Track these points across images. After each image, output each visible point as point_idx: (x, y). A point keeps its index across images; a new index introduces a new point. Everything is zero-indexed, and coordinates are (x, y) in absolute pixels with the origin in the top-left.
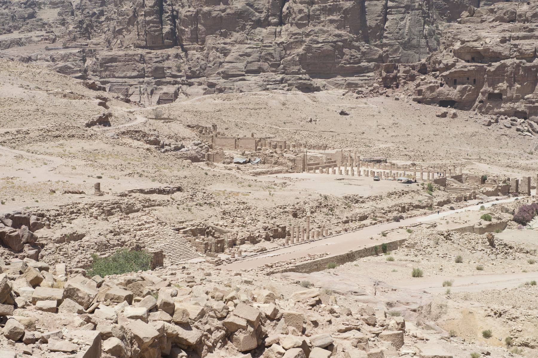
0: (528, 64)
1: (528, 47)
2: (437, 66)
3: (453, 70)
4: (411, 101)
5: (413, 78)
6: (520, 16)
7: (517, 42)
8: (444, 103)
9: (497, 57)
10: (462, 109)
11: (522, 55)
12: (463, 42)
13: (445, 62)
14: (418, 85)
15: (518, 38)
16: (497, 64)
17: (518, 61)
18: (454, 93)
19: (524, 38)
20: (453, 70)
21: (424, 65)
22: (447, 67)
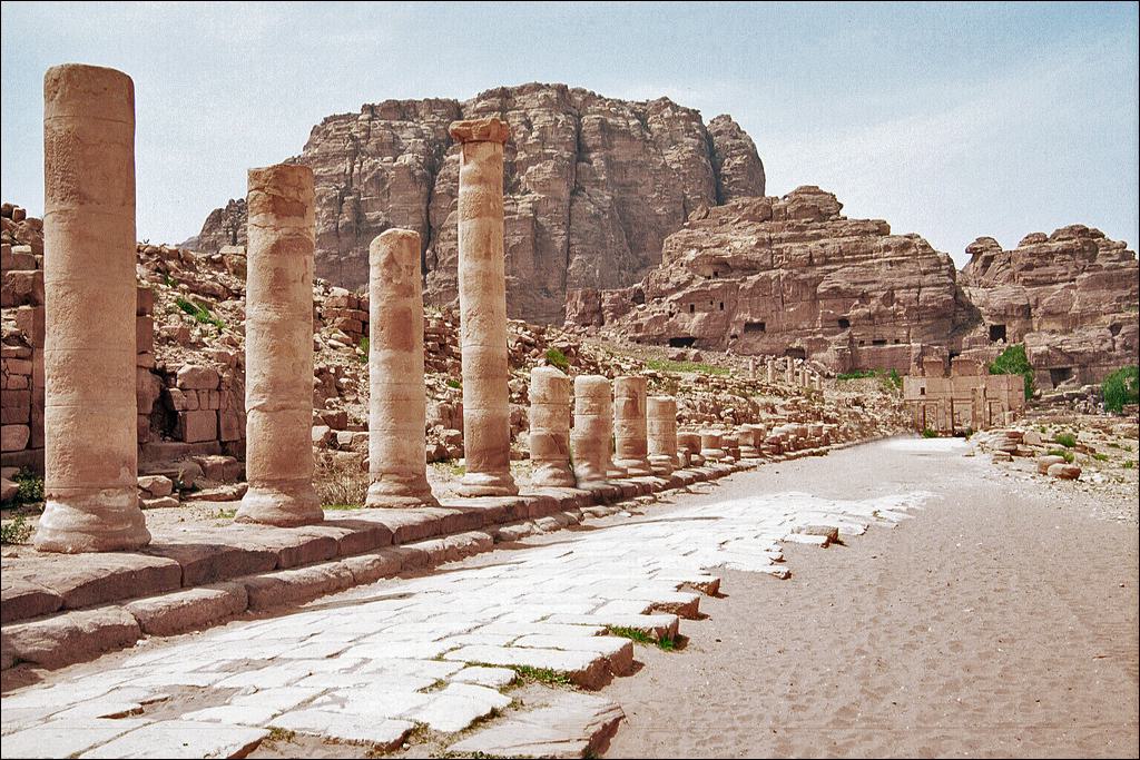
0: (802, 276)
1: (798, 251)
2: (664, 287)
3: (688, 290)
4: (626, 341)
5: (624, 310)
6: (779, 211)
7: (781, 246)
8: (676, 342)
9: (751, 267)
10: (706, 348)
11: (792, 263)
12: (701, 249)
13: (675, 280)
14: (636, 317)
15: (780, 240)
16: (756, 278)
17: (786, 272)
18: (692, 323)
19: (791, 239)
20: (688, 290)
21: (640, 290)
22: (679, 287)
